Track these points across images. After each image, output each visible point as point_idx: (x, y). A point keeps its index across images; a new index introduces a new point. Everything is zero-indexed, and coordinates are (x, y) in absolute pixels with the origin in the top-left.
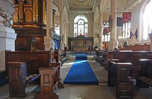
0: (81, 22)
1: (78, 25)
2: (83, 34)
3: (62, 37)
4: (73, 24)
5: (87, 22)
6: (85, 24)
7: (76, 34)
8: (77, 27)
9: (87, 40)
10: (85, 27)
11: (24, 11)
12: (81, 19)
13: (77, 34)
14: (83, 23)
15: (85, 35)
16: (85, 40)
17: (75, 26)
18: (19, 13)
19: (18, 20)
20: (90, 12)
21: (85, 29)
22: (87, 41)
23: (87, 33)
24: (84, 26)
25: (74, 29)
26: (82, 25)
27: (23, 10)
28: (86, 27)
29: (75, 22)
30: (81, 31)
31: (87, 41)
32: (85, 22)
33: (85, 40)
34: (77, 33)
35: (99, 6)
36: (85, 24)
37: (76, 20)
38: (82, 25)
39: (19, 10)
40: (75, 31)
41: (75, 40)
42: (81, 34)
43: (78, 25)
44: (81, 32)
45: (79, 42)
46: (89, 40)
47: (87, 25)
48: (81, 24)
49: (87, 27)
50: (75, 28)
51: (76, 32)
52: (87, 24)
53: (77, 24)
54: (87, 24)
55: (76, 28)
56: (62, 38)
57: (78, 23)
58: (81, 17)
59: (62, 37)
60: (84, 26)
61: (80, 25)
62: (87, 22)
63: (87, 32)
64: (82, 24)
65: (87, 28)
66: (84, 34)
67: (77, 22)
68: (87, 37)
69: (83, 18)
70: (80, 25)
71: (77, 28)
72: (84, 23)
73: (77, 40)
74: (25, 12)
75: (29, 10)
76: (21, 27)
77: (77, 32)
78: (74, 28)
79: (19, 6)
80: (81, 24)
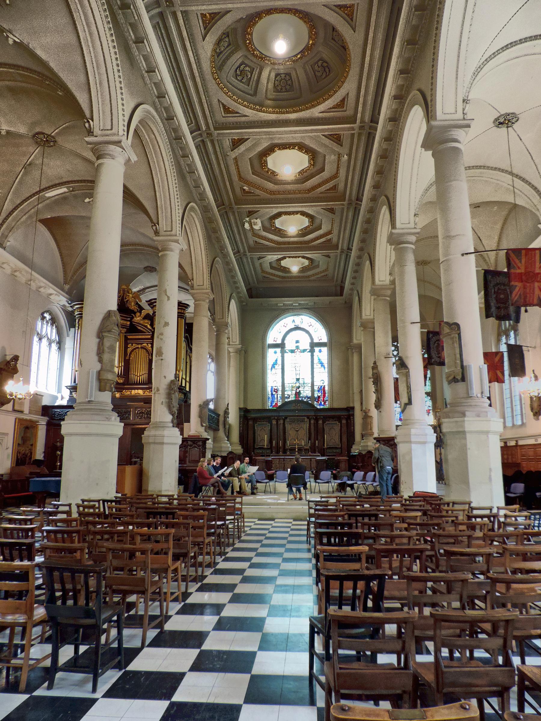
0: (297, 342)
1: (286, 354)
2: (306, 392)
3: (221, 413)
4: (263, 348)
5: (325, 339)
6: (317, 349)
7: (276, 391)
8: (279, 362)
9: (326, 419)
10: (316, 361)
11: (129, 350)
12: (297, 328)
13: (280, 393)
14: (305, 344)
15: (316, 396)
16: (317, 420)
17: (272, 355)
20: (339, 299)
21: (317, 366)
22: (324, 422)
23: (326, 388)
24: (312, 356)
25: (269, 371)
26: (304, 351)
27: (126, 348)
28: (322, 365)
30: (298, 380)
31: (324, 422)
32: (316, 340)
33: (317, 420)
35: (360, 293)
36: (317, 349)
38: (304, 351)
41: (269, 419)
42: (298, 394)
44: (298, 385)
45: (288, 426)
46: (333, 417)
47: (323, 354)
48: (297, 347)
49: (325, 361)
50: (273, 366)
51: (274, 385)
52: (325, 350)
54: (325, 350)
55: (276, 366)
56: (221, 419)
57: (281, 346)
59: (221, 413)
60: (312, 356)
61: (292, 351)
62: (325, 339)
63: (326, 384)
64: (302, 348)
65: (326, 366)
66: (313, 391)
67: (279, 341)
68: (327, 406)
70: (292, 351)
71: (279, 367)
72: (313, 345)
73: (282, 422)
74: (130, 353)
75: (142, 348)
78: (269, 366)
80: (297, 347)
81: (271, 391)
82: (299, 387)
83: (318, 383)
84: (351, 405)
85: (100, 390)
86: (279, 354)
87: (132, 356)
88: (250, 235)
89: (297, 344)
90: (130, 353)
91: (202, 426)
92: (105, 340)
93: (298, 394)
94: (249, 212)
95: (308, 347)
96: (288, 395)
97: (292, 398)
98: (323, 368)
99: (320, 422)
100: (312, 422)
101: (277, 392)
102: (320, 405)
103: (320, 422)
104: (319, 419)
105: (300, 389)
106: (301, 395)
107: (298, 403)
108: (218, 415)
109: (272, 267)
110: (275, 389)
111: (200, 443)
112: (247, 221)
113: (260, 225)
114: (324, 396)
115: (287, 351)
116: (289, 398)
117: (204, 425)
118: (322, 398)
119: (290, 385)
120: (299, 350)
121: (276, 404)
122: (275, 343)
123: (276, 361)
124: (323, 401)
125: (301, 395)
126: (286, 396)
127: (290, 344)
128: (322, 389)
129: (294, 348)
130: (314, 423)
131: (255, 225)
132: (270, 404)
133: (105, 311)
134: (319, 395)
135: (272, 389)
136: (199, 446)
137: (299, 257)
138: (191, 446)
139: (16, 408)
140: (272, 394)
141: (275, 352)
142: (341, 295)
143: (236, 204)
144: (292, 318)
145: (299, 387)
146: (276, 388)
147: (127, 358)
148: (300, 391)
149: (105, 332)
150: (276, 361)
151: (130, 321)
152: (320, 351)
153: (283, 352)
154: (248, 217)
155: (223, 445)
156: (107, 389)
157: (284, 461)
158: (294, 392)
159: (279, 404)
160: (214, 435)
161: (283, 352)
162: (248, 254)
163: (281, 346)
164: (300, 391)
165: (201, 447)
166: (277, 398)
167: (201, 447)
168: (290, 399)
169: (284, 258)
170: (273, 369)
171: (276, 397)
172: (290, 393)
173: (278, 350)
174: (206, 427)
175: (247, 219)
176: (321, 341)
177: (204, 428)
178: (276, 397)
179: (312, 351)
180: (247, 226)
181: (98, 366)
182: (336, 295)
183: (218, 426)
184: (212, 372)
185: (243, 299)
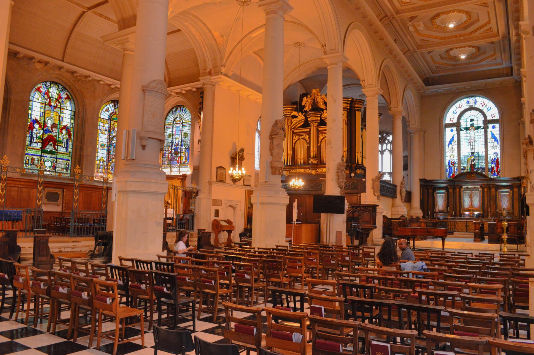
0: (472, 120)
1: (461, 132)
2: (481, 164)
4: (441, 128)
5: (497, 117)
6: (490, 126)
7: (453, 164)
8: (456, 139)
10: (489, 135)
11: (320, 139)
12: (471, 108)
14: (479, 121)
16: (490, 188)
17: (449, 134)
18: (309, 145)
19: (308, 160)
25: (447, 147)
26: (478, 128)
27: (318, 137)
28: (495, 139)
29: (447, 121)
32: (489, 118)
33: (490, 188)
34: (456, 161)
36: (490, 126)
37: (451, 116)
38: (478, 128)
39: (309, 138)
40: (450, 155)
42: (473, 166)
43: (458, 134)
44: (472, 158)
47: (495, 130)
48: (472, 125)
49: (498, 136)
50: (450, 143)
52: (497, 125)
53: (455, 129)
54: (497, 125)
55: (453, 143)
57: (457, 125)
58: (471, 100)
61: (467, 129)
62: (497, 117)
63: (499, 156)
67: (455, 121)
69: (480, 101)
70: (467, 129)
71: (455, 143)
72: (486, 122)
74: (321, 141)
76: (314, 172)
77: (456, 159)
78: (447, 143)
79: (310, 131)
80: (472, 125)
82: (474, 160)
83: (491, 155)
84: (523, 175)
85: (272, 174)
86: (455, 132)
87: (323, 143)
88: (415, 35)
89: (471, 123)
90: (321, 141)
91: (375, 195)
92: (274, 140)
93: (473, 166)
94: (411, 18)
95: (481, 124)
96: (464, 167)
97: (468, 170)
98: (496, 143)
99: (493, 190)
100: (486, 190)
101: (453, 165)
102: (494, 175)
103: (493, 190)
104: (492, 187)
105: (475, 162)
106: (476, 167)
107: (472, 174)
108: (396, 186)
109: (442, 58)
110: (452, 162)
111: (371, 208)
112: (410, 25)
113: (423, 26)
114: (498, 167)
115: (463, 129)
116: (465, 169)
117: (376, 194)
118: (495, 169)
119: (466, 158)
120: (473, 128)
121: (453, 175)
122: (451, 122)
123: (453, 138)
124: (497, 172)
125: (476, 167)
126: (462, 167)
127: (465, 123)
128: (495, 161)
129: (469, 126)
130: (487, 191)
131: (418, 26)
132: (447, 175)
133: (274, 120)
134: (493, 166)
135: (449, 162)
136: (370, 211)
137: (465, 47)
138: (363, 210)
139: (245, 183)
140: (449, 167)
141: (452, 131)
142: (512, 75)
143: (397, 13)
144: (465, 100)
145: (474, 160)
146: (453, 161)
147: (319, 145)
148: (474, 163)
149: (274, 135)
150: (453, 138)
151: (320, 117)
152: (493, 127)
153: (459, 130)
154: (410, 21)
155: (400, 210)
156: (277, 173)
157: (455, 223)
158: (469, 164)
159: (456, 175)
160: (393, 201)
161: (459, 130)
162: (418, 51)
163: (457, 125)
164: (474, 163)
165: (371, 212)
166: (454, 170)
167: (371, 212)
168: (466, 171)
169: (452, 49)
170: (450, 146)
171: (453, 169)
172: (465, 165)
173: (455, 129)
174: (378, 196)
175: (410, 23)
176: (494, 118)
177: (376, 197)
178: (453, 169)
179: (486, 128)
180: (411, 28)
181: (271, 158)
182: (507, 75)
183: (396, 194)
184: (388, 150)
185: (419, 88)
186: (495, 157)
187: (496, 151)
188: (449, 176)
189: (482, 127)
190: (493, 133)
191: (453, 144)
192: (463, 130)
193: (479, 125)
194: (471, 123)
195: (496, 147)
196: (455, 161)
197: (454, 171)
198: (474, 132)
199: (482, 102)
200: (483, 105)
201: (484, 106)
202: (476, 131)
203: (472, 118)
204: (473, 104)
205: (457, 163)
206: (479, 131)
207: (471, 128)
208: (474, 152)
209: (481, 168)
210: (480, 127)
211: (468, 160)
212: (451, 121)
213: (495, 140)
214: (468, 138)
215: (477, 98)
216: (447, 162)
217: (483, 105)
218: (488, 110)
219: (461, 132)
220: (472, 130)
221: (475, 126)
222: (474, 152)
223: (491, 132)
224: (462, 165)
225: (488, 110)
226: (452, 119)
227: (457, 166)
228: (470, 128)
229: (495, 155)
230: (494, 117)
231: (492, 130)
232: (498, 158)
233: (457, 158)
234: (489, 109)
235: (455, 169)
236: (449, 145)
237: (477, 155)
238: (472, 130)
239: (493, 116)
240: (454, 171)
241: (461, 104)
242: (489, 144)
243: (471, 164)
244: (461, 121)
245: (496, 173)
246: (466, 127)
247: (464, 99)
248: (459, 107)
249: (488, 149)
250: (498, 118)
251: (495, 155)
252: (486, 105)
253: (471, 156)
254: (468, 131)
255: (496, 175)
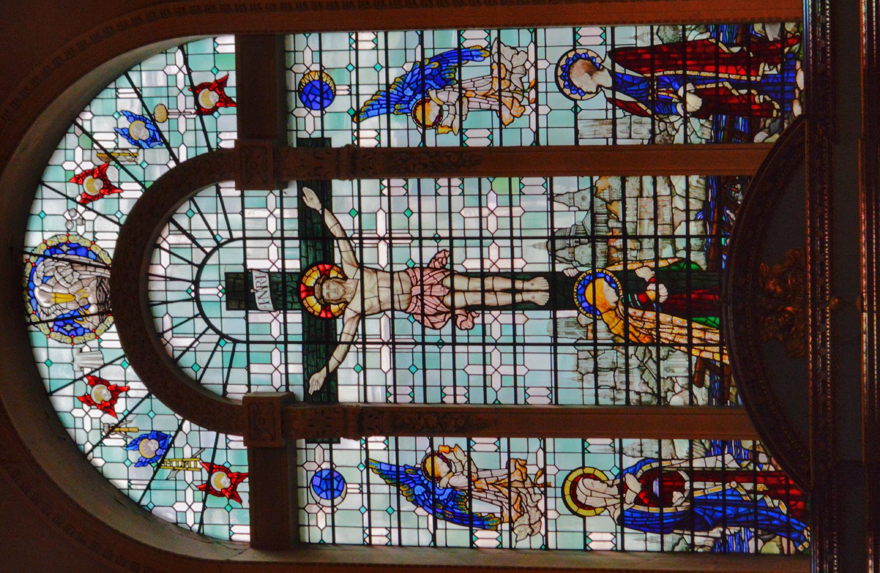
25: (486, 539)
81: (661, 526)
89: (263, 297)
96: (694, 379)
98: (470, 72)
105: (645, 273)
106: (699, 259)
115: (318, 380)
119: (608, 357)
122: (243, 488)
124: (751, 67)
125: (699, 259)
126: (701, 395)
134: (694, 102)
135: (643, 524)
146: (634, 485)
164: (660, 276)
170: (478, 507)
171: (713, 488)
176: (231, 91)
178: (713, 488)
186: (605, 79)
187: (547, 72)
188: (785, 530)
189: (313, 201)
190: (367, 92)
191: (461, 481)
192: (332, 378)
193: (292, 227)
194: (263, 297)
195: (500, 72)
196: (628, 462)
197: (740, 475)
198: (350, 271)
199: (73, 190)
200: (109, 188)
201: (112, 174)
202: (342, 253)
203: (211, 292)
204: (87, 274)
205: (650, 447)
206: (348, 223)
207: (312, 300)
208: (552, 277)
209: (706, 213)
210: (303, 210)
211: (622, 342)
212: (232, 493)
213: (443, 83)
214: (406, 328)
215: (35, 240)
216: (634, 541)
217: (109, 188)
218: (157, 138)
219: (347, 394)
220: (331, 291)
221: (293, 265)
222: (552, 277)
223: (357, 115)
224: (677, 401)
225: (157, 138)
226: (221, 481)
227: (682, 447)
228: (308, 315)
229: (580, 77)
230: (219, 86)
231: (342, 103)
232: (619, 55)
233: (599, 444)
234: (141, 132)
235: (712, 462)
236: (472, 521)
237: (584, 253)
238: (331, 291)
239: (209, 99)
240: (740, 475)
241: (82, 388)
242: (477, 139)
243: (669, 307)
244: (237, 391)
245: (765, 69)
246: (296, 352)
247: (42, 355)
248: (108, 408)
249: (528, 140)
250: (227, 44)
251: (580, 77)
252: (109, 156)
253: (592, 310)
254: (345, 328)
255: (788, 70)
